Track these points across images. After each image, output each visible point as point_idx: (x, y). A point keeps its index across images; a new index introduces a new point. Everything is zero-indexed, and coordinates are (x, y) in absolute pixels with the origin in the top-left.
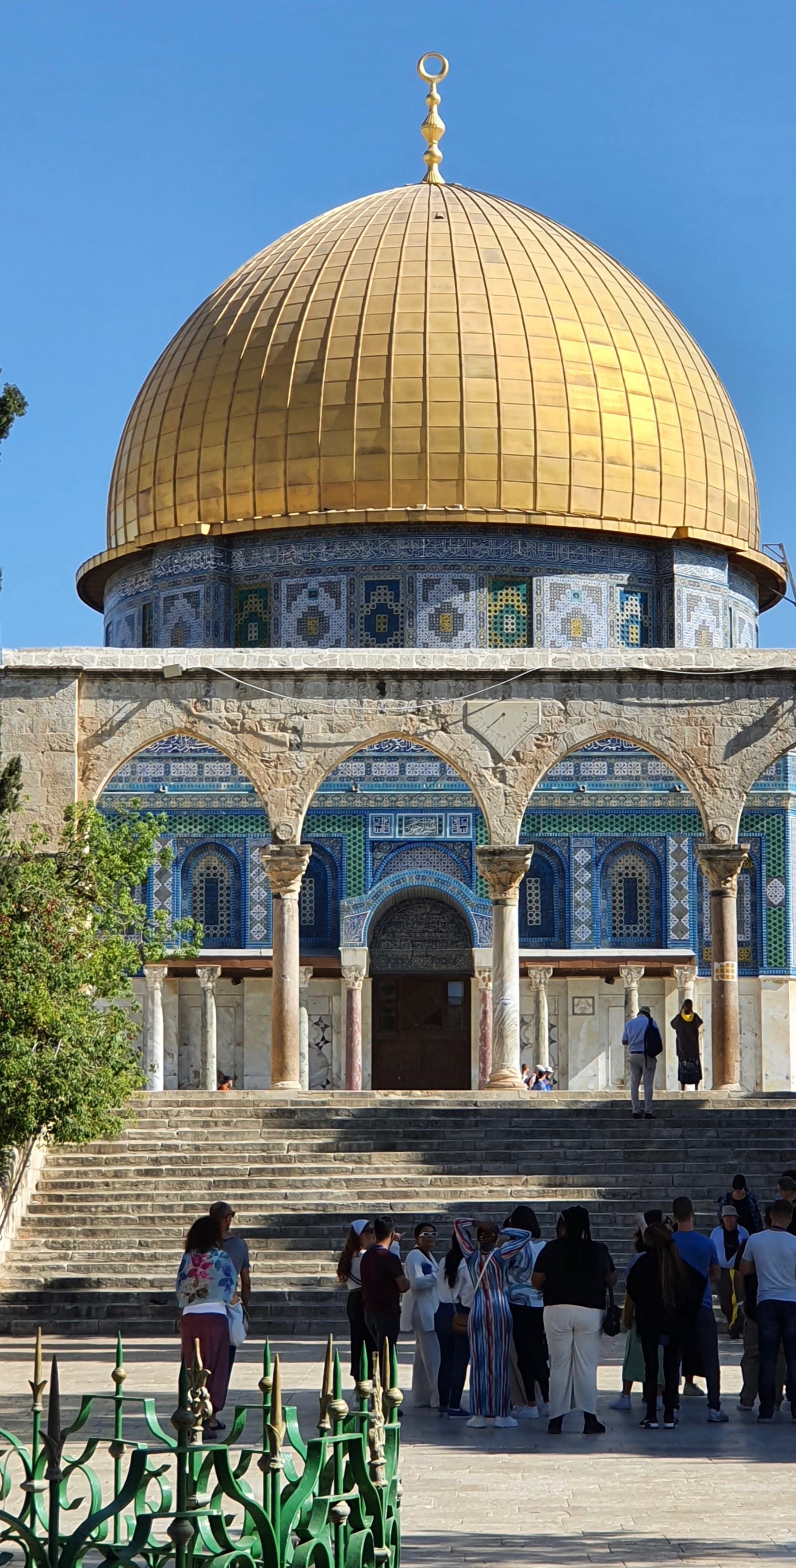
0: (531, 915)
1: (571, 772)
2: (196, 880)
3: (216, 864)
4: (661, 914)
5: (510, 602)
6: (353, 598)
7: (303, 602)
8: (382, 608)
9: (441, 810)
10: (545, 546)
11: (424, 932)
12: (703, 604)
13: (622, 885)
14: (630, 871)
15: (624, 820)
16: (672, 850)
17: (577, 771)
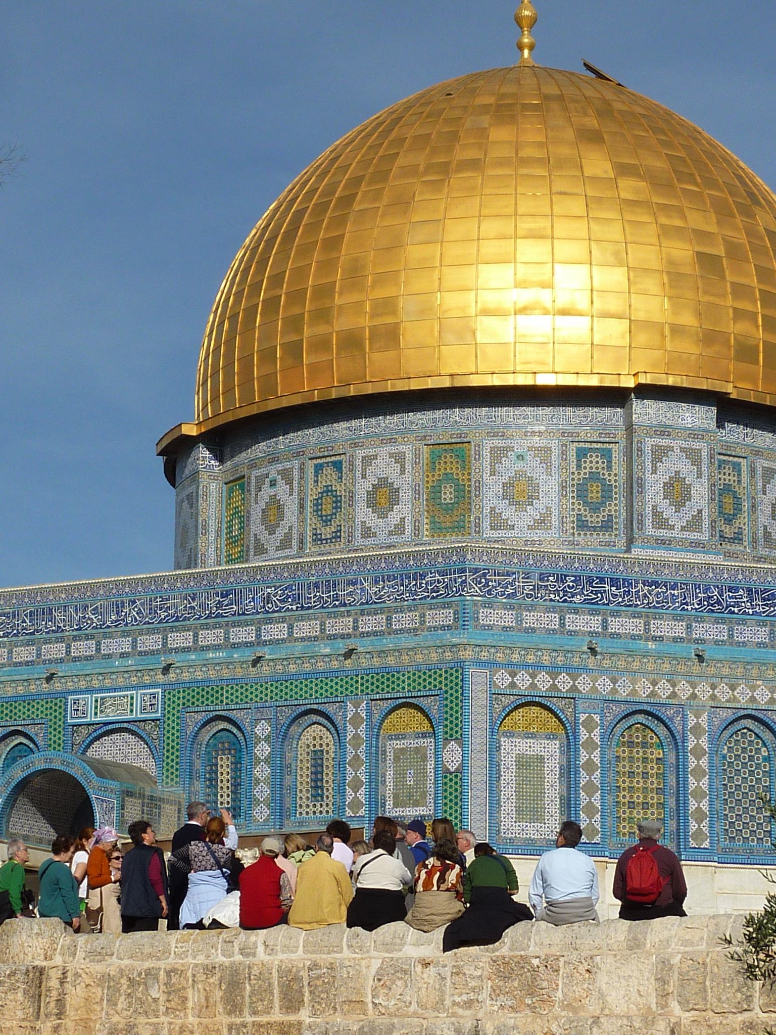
1: (252, 638)
5: (448, 471)
7: (267, 492)
8: (328, 490)
9: (133, 687)
15: (303, 686)
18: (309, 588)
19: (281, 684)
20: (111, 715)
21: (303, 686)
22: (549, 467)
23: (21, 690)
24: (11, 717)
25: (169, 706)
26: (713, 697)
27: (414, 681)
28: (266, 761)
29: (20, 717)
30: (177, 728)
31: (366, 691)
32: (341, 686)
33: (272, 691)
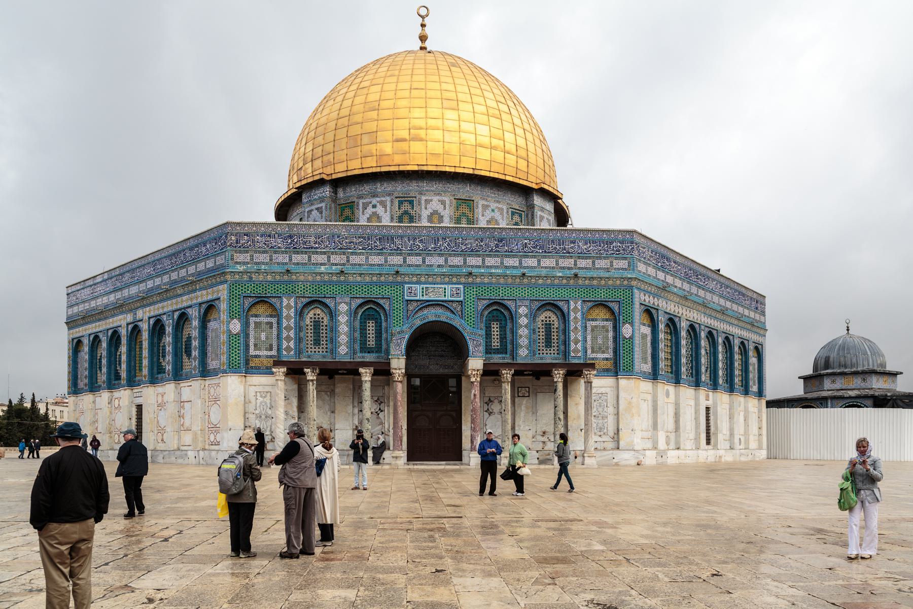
0: (494, 342)
2: (308, 321)
3: (319, 313)
4: (566, 343)
6: (392, 207)
7: (370, 210)
8: (406, 213)
9: (446, 284)
10: (479, 188)
11: (435, 351)
12: (545, 220)
13: (543, 327)
14: (548, 319)
15: (546, 291)
16: (572, 307)
17: (520, 263)
18: (549, 242)
19: (534, 289)
20: (432, 297)
21: (546, 291)
22: (503, 215)
23: (375, 279)
24: (368, 293)
25: (468, 295)
26: (686, 315)
27: (607, 293)
28: (526, 326)
29: (374, 293)
30: (473, 306)
31: (581, 296)
32: (567, 293)
33: (528, 292)
